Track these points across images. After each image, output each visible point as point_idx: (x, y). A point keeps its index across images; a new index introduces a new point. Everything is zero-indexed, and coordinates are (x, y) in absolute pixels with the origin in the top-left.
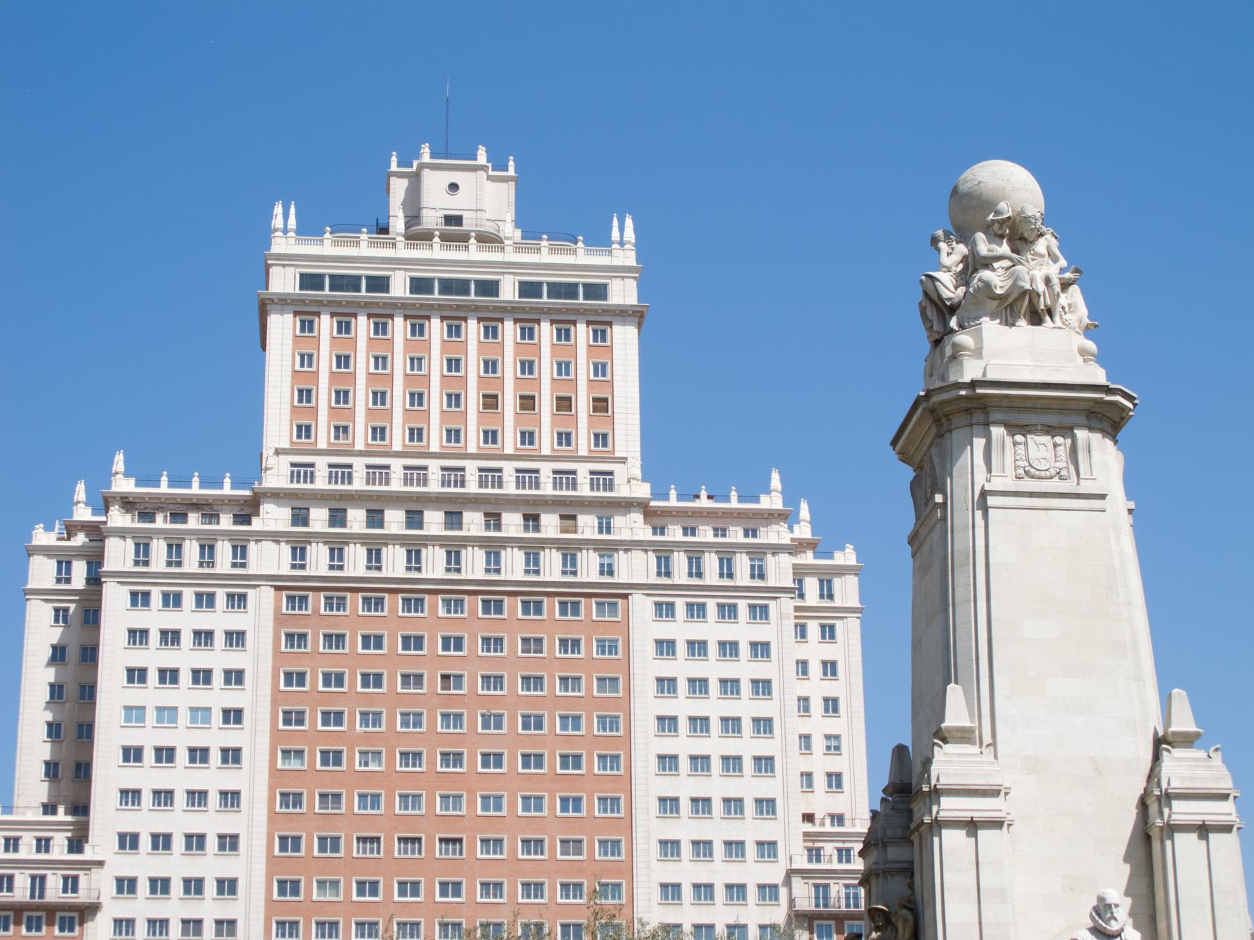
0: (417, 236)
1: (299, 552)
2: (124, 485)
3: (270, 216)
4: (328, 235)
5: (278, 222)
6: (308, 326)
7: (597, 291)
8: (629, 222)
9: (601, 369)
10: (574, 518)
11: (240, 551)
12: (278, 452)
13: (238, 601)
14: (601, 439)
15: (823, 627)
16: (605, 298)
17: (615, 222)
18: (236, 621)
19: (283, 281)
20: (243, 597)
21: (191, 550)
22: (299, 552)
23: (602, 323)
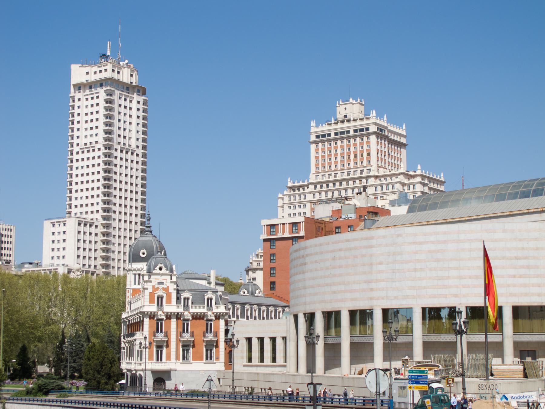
0: (336, 123)
1: (314, 194)
2: (290, 184)
3: (311, 124)
4: (320, 126)
5: (312, 125)
6: (317, 146)
7: (367, 129)
8: (374, 112)
9: (369, 146)
10: (362, 180)
11: (305, 196)
12: (313, 174)
13: (305, 206)
14: (369, 162)
15: (413, 196)
16: (369, 130)
17: (371, 112)
18: (305, 210)
19: (313, 138)
20: (305, 205)
21: (297, 197)
22: (314, 194)
23: (368, 136)
